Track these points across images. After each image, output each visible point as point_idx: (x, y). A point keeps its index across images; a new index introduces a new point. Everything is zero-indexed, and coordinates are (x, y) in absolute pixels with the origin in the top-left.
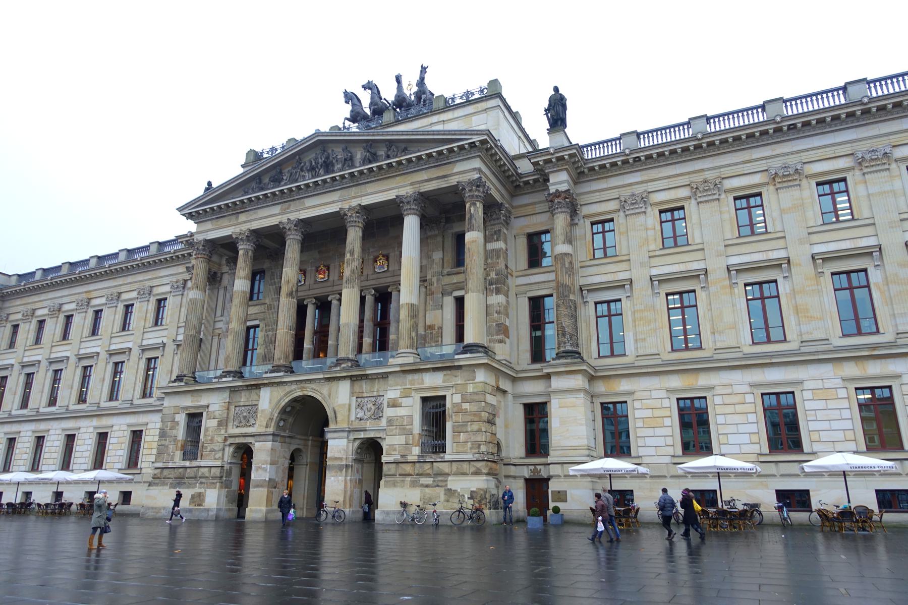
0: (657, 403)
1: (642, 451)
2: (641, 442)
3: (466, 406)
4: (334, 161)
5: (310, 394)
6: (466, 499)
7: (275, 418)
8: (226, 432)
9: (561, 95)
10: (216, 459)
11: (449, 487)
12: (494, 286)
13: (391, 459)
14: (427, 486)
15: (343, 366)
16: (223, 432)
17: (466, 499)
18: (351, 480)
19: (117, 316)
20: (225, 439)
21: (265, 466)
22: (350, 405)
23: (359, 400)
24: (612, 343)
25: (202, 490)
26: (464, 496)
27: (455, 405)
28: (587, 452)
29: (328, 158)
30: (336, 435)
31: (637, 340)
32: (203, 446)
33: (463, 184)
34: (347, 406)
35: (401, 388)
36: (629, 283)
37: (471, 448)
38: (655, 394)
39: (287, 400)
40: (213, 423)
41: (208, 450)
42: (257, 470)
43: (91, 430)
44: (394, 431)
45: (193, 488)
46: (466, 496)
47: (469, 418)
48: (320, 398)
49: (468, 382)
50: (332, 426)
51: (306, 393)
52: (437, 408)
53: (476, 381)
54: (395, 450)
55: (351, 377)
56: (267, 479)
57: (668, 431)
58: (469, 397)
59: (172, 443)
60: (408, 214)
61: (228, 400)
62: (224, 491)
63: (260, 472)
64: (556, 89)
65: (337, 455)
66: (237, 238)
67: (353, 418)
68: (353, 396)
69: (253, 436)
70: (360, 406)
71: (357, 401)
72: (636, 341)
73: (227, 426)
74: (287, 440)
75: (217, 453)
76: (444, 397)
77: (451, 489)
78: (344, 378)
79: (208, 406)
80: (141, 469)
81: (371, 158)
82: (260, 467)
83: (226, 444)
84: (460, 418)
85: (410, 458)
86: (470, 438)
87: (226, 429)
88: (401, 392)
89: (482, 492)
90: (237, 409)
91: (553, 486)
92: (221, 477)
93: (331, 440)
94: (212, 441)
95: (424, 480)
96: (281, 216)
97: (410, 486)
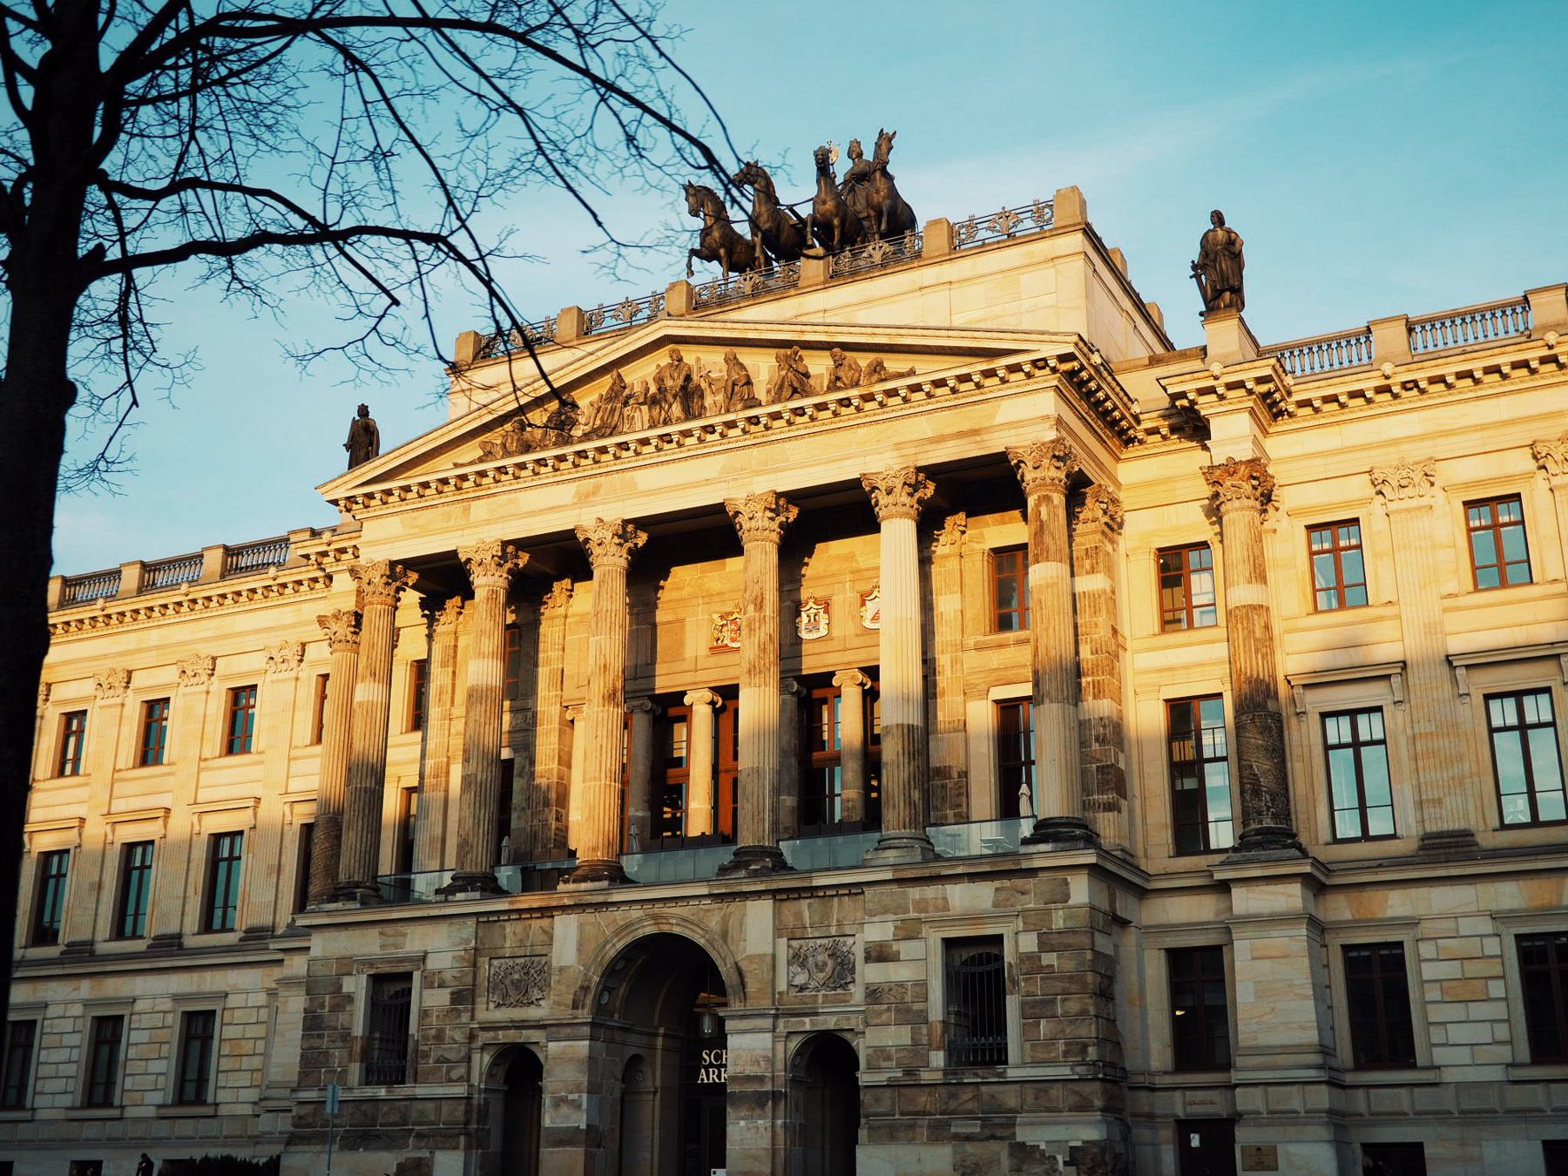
0: (1471, 946)
1: (1440, 1056)
2: (1437, 1035)
3: (1050, 959)
4: (704, 385)
5: (677, 930)
6: (1061, 1166)
7: (593, 986)
8: (472, 1018)
9: (1229, 232)
10: (450, 1080)
11: (1019, 1139)
12: (1090, 679)
13: (881, 1078)
14: (969, 1138)
15: (752, 867)
16: (465, 1018)
17: (1061, 1166)
18: (785, 1125)
19: (125, 730)
20: (472, 1037)
21: (574, 1096)
22: (774, 956)
23: (795, 944)
24: (1363, 808)
25: (425, 1154)
26: (1055, 1158)
27: (1026, 958)
28: (1316, 1059)
29: (688, 378)
30: (745, 1024)
31: (1421, 803)
32: (416, 1051)
33: (1020, 451)
34: (769, 959)
35: (894, 917)
36: (1399, 670)
37: (1066, 1053)
38: (1466, 926)
39: (620, 945)
40: (438, 999)
43: (77, 1010)
44: (884, 1017)
45: (400, 1148)
46: (1060, 1159)
47: (1059, 986)
48: (701, 942)
49: (1053, 906)
50: (736, 1006)
51: (666, 928)
52: (981, 964)
53: (1071, 902)
54: (888, 1058)
55: (774, 893)
56: (583, 1126)
57: (1499, 1010)
58: (1055, 940)
59: (339, 1044)
60: (891, 516)
61: (473, 944)
62: (476, 1154)
63: (564, 1109)
64: (1218, 218)
65: (750, 1070)
66: (469, 560)
67: (782, 986)
68: (780, 936)
69: (544, 1027)
70: (798, 959)
71: (789, 946)
72: (1420, 804)
73: (473, 1003)
74: (619, 1036)
75: (453, 1068)
76: (998, 940)
77: (1024, 1143)
78: (759, 894)
79: (424, 958)
80: (216, 1105)
81: (796, 385)
82: (564, 1100)
83: (473, 1046)
84: (1038, 988)
85: (926, 1076)
86: (1063, 1031)
87: (473, 1010)
88: (896, 928)
89: (1095, 1150)
90: (495, 962)
91: (1244, 1136)
92: (467, 1122)
93: (735, 1036)
94: (439, 1037)
95: (958, 1128)
97: (928, 1139)
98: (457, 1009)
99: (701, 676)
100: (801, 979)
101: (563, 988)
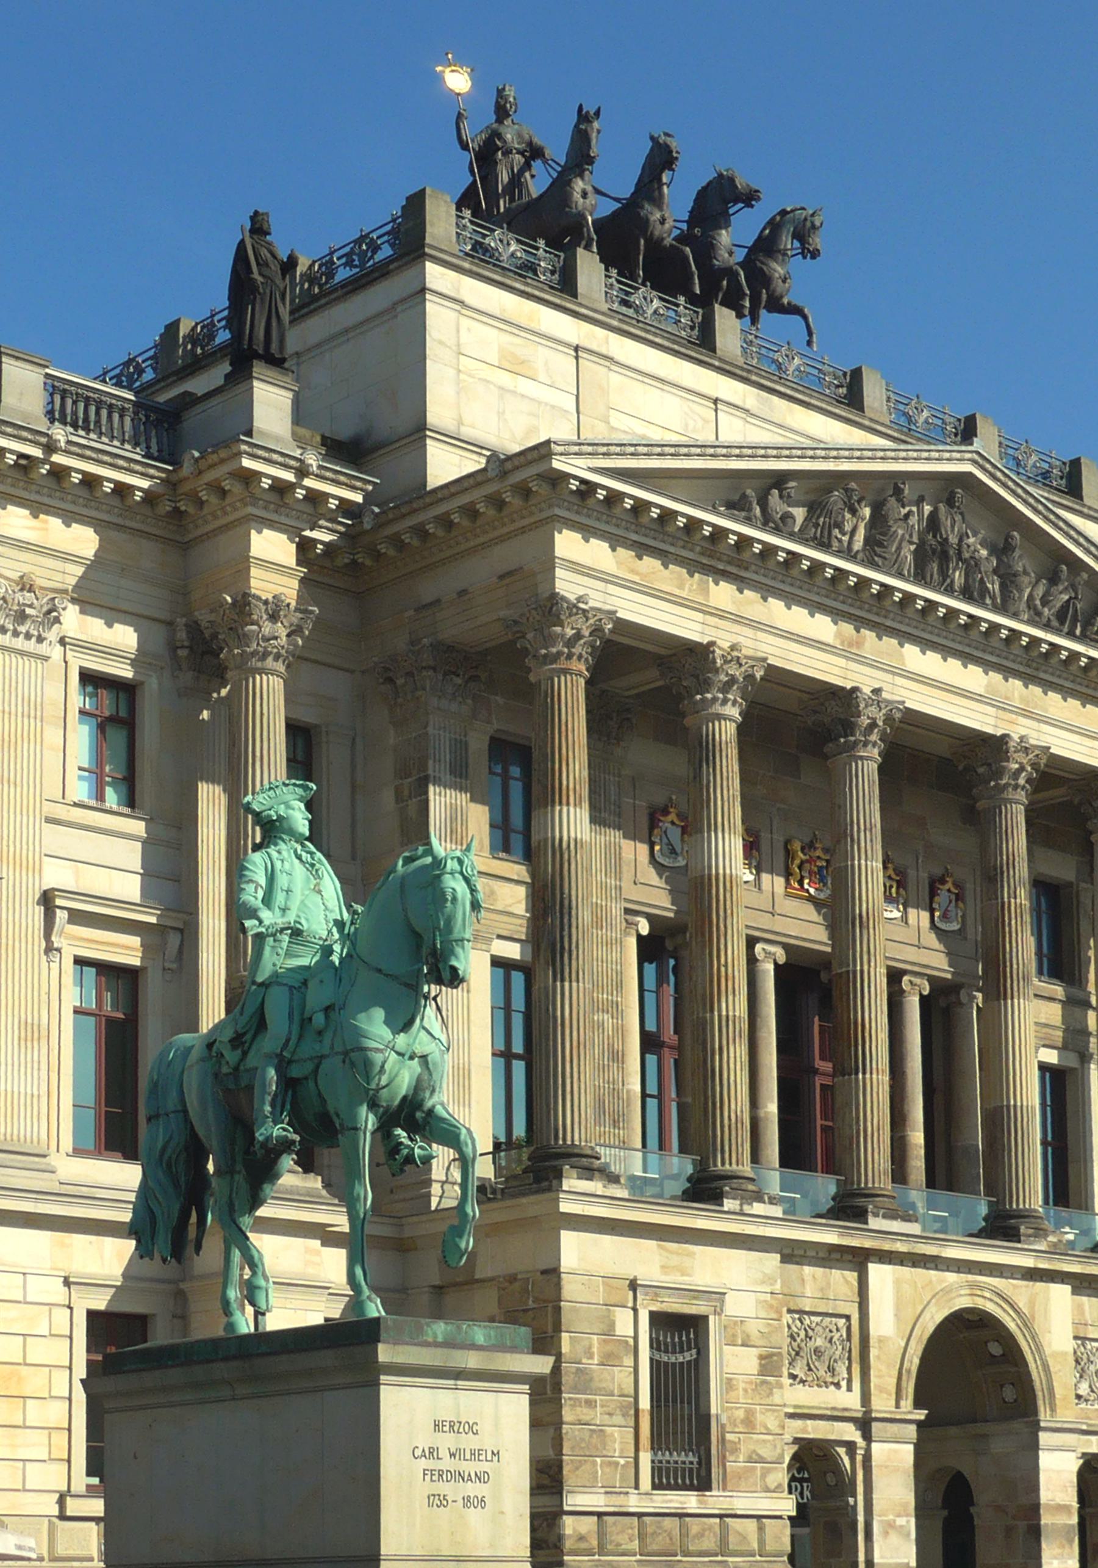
32: (723, 1441)
41: (741, 1459)
42: (886, 1533)
59: (618, 1419)
75: (769, 1470)
94: (749, 1422)
96: (842, 662)
98: (764, 1382)
99: (780, 925)
100: (1084, 1389)
101: (883, 1368)
